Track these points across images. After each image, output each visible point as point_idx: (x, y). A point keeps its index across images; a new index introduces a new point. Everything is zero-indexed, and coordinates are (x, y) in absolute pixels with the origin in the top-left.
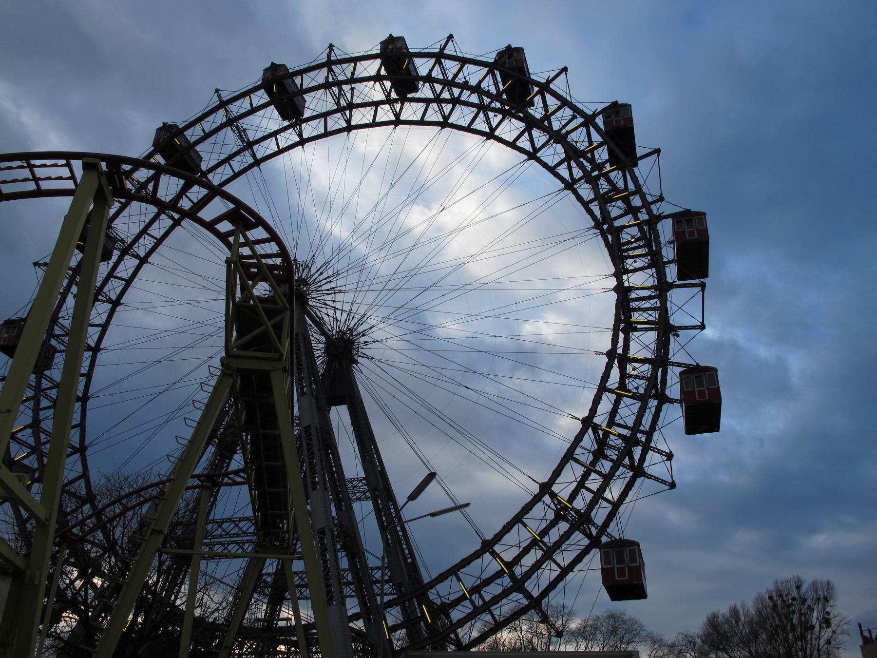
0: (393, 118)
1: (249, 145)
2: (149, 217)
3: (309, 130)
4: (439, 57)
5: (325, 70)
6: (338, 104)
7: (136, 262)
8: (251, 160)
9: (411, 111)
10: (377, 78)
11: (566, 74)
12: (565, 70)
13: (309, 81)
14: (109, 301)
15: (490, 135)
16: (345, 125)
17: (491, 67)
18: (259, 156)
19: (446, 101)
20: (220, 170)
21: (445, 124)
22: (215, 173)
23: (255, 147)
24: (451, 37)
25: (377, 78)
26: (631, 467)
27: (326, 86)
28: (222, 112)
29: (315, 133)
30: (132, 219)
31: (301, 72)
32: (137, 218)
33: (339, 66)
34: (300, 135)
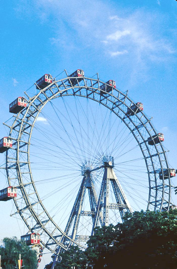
1: (151, 157)
2: (135, 123)
5: (168, 185)
6: (158, 186)
7: (122, 117)
8: (146, 156)
14: (113, 108)
18: (147, 159)
20: (145, 147)
22: (144, 145)
23: (150, 158)
26: (47, 244)
28: (162, 151)
29: (151, 178)
30: (135, 119)
32: (135, 121)
33: (169, 189)
34: (151, 173)
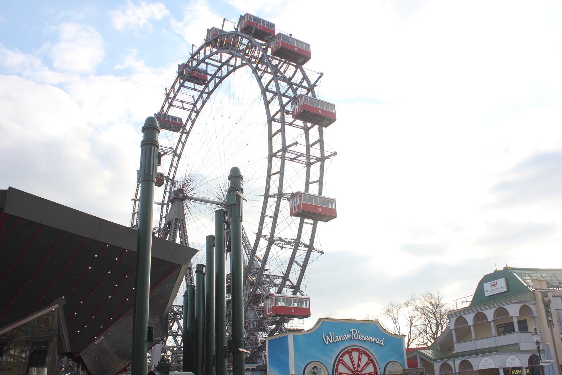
0: (207, 95)
3: (188, 128)
4: (192, 58)
9: (211, 86)
10: (182, 86)
11: (227, 21)
12: (225, 19)
13: (165, 109)
15: (235, 68)
16: (195, 114)
17: (207, 44)
19: (217, 71)
21: (222, 79)
24: (193, 45)
25: (182, 86)
27: (171, 105)
31: (162, 108)
